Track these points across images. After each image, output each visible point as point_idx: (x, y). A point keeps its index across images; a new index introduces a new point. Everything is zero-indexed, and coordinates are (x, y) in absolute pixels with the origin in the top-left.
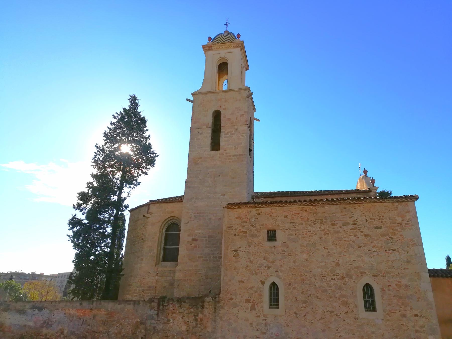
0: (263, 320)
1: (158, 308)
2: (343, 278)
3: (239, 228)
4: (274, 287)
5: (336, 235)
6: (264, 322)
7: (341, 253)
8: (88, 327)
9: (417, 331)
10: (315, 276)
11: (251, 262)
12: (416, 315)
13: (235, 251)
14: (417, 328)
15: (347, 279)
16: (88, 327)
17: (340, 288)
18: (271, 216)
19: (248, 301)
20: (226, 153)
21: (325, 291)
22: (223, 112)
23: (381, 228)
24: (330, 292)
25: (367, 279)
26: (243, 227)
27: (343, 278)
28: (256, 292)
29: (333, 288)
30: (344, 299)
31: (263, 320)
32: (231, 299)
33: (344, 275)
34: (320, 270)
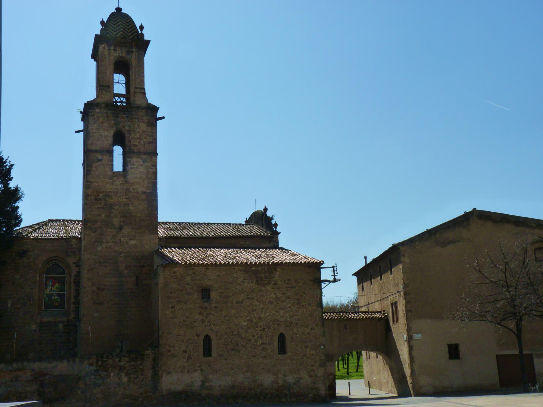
0: (199, 367)
1: (97, 363)
2: (264, 329)
3: (175, 286)
4: (207, 338)
5: (260, 294)
6: (199, 368)
7: (263, 308)
8: (9, 389)
9: (312, 366)
10: (241, 328)
11: (187, 317)
12: (313, 355)
13: (172, 307)
14: (313, 364)
15: (267, 330)
16: (9, 389)
17: (261, 338)
18: (205, 275)
19: (185, 351)
20: (133, 189)
21: (250, 340)
22: (127, 135)
23: (295, 287)
24: (253, 340)
25: (282, 330)
26: (179, 285)
27: (264, 329)
28: (192, 343)
29: (256, 337)
30: (263, 346)
31: (199, 367)
32: (169, 351)
33: (265, 327)
34: (245, 324)
